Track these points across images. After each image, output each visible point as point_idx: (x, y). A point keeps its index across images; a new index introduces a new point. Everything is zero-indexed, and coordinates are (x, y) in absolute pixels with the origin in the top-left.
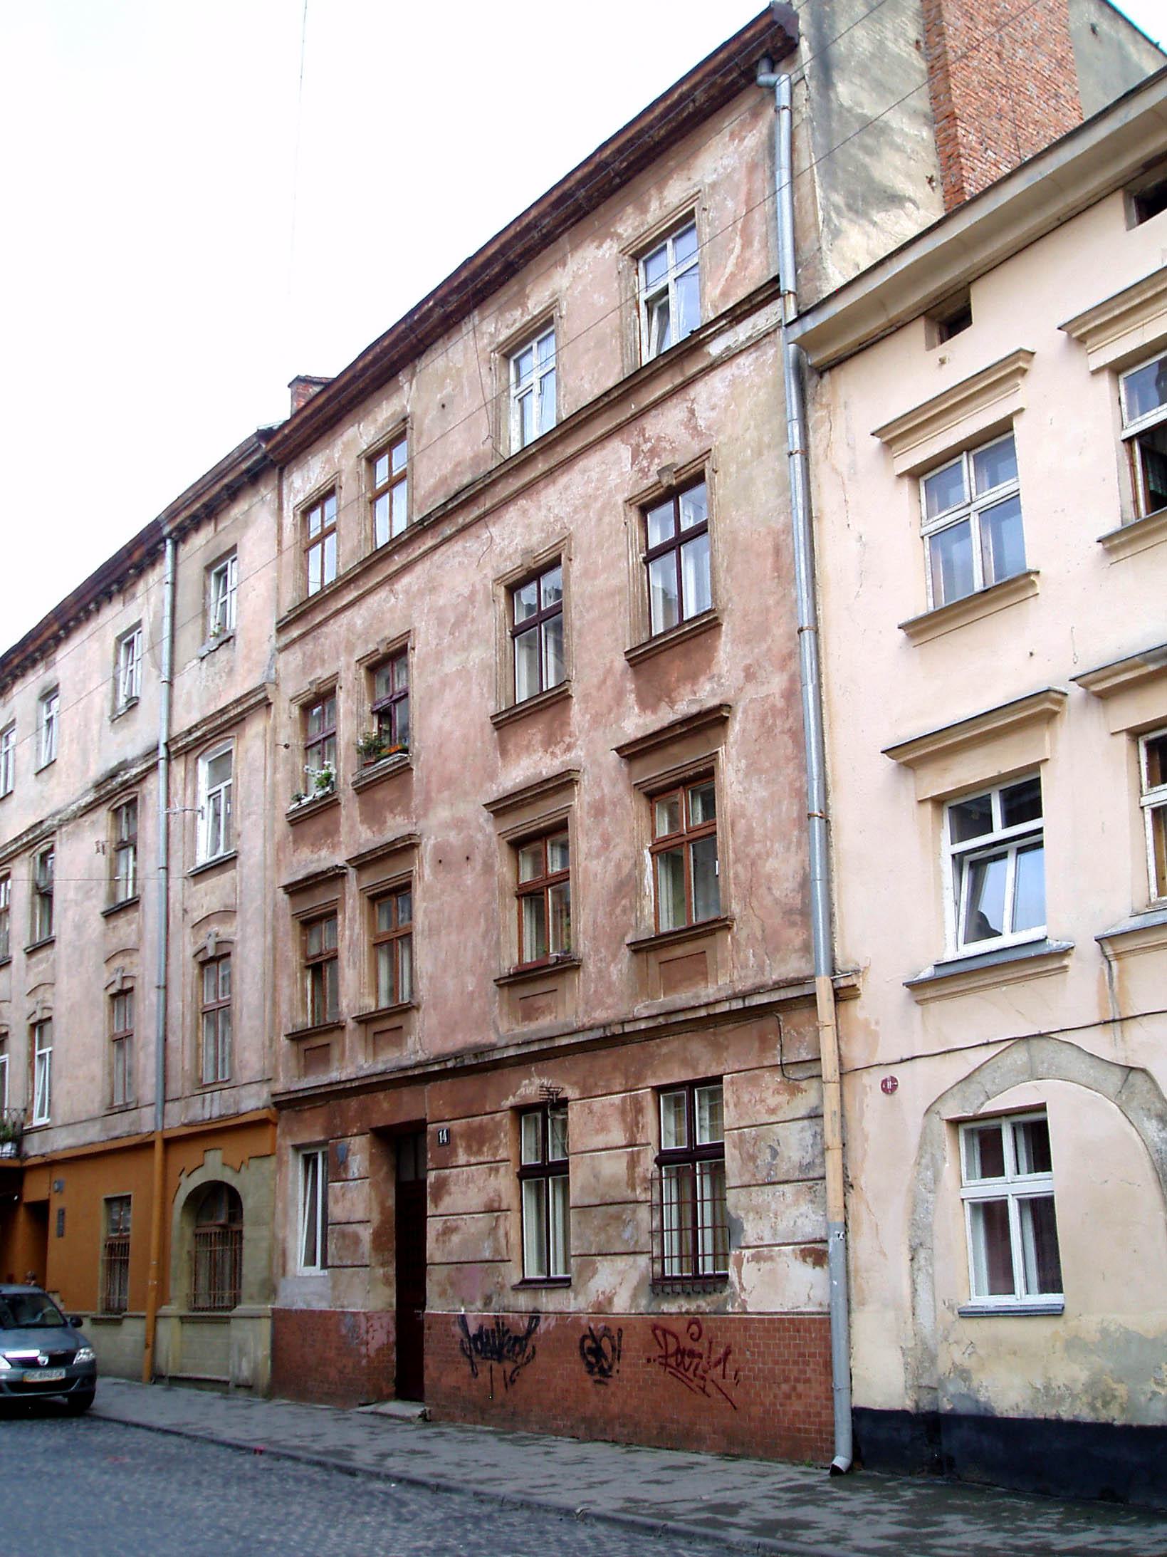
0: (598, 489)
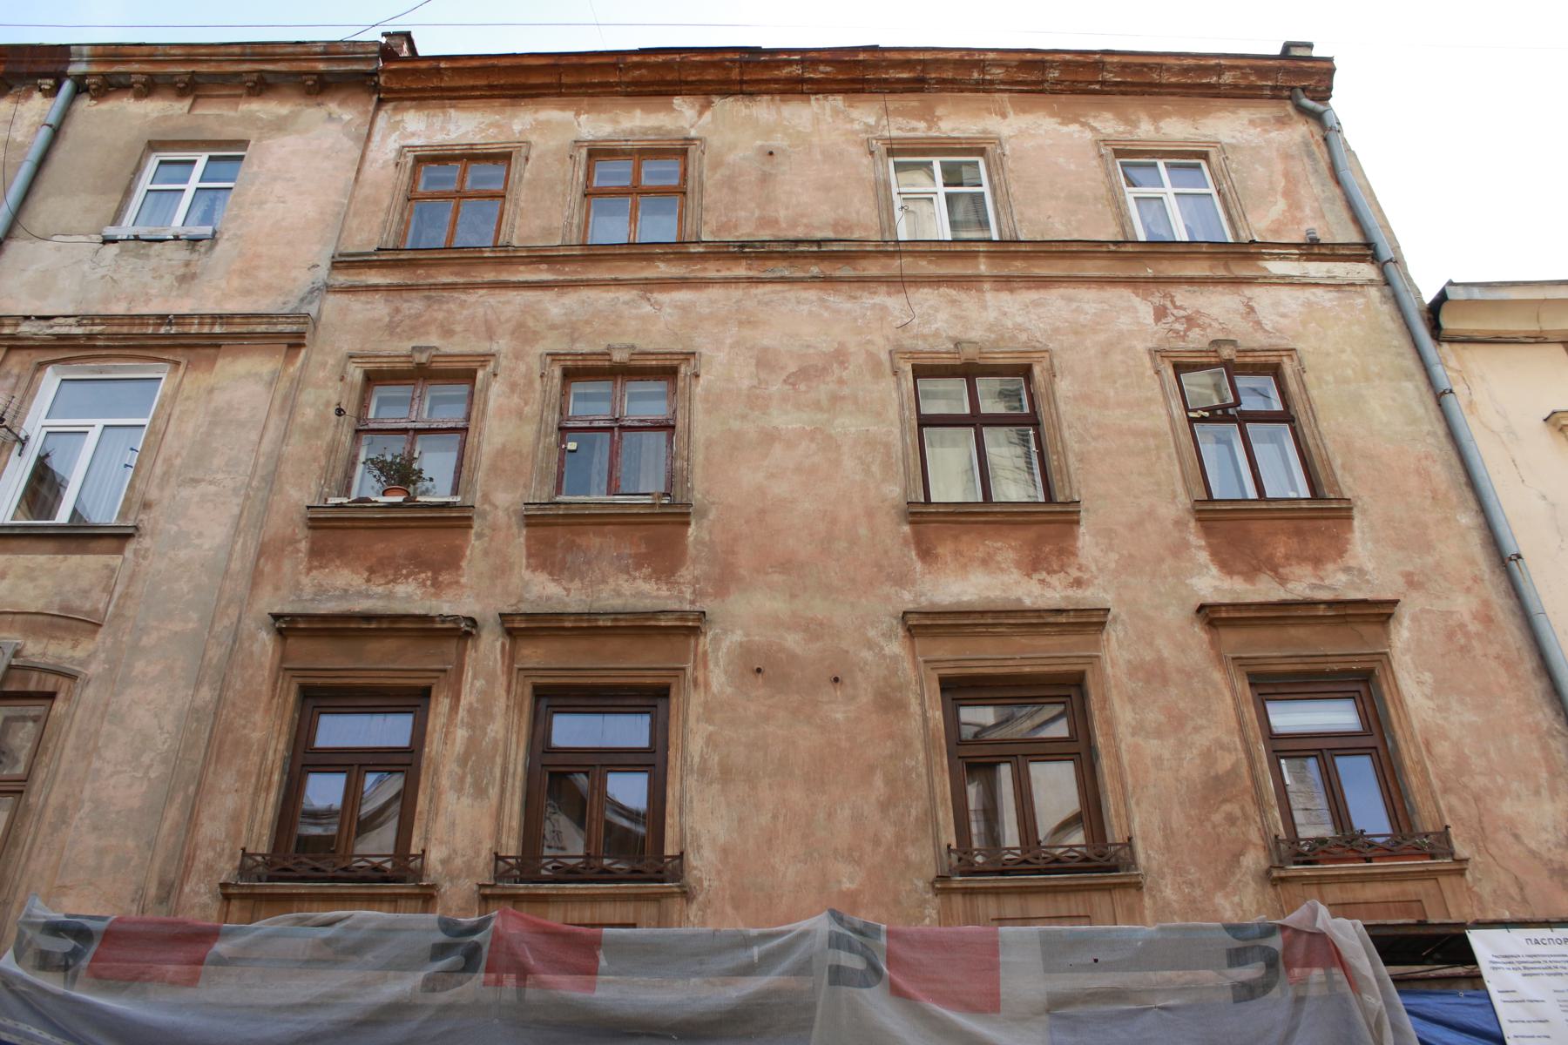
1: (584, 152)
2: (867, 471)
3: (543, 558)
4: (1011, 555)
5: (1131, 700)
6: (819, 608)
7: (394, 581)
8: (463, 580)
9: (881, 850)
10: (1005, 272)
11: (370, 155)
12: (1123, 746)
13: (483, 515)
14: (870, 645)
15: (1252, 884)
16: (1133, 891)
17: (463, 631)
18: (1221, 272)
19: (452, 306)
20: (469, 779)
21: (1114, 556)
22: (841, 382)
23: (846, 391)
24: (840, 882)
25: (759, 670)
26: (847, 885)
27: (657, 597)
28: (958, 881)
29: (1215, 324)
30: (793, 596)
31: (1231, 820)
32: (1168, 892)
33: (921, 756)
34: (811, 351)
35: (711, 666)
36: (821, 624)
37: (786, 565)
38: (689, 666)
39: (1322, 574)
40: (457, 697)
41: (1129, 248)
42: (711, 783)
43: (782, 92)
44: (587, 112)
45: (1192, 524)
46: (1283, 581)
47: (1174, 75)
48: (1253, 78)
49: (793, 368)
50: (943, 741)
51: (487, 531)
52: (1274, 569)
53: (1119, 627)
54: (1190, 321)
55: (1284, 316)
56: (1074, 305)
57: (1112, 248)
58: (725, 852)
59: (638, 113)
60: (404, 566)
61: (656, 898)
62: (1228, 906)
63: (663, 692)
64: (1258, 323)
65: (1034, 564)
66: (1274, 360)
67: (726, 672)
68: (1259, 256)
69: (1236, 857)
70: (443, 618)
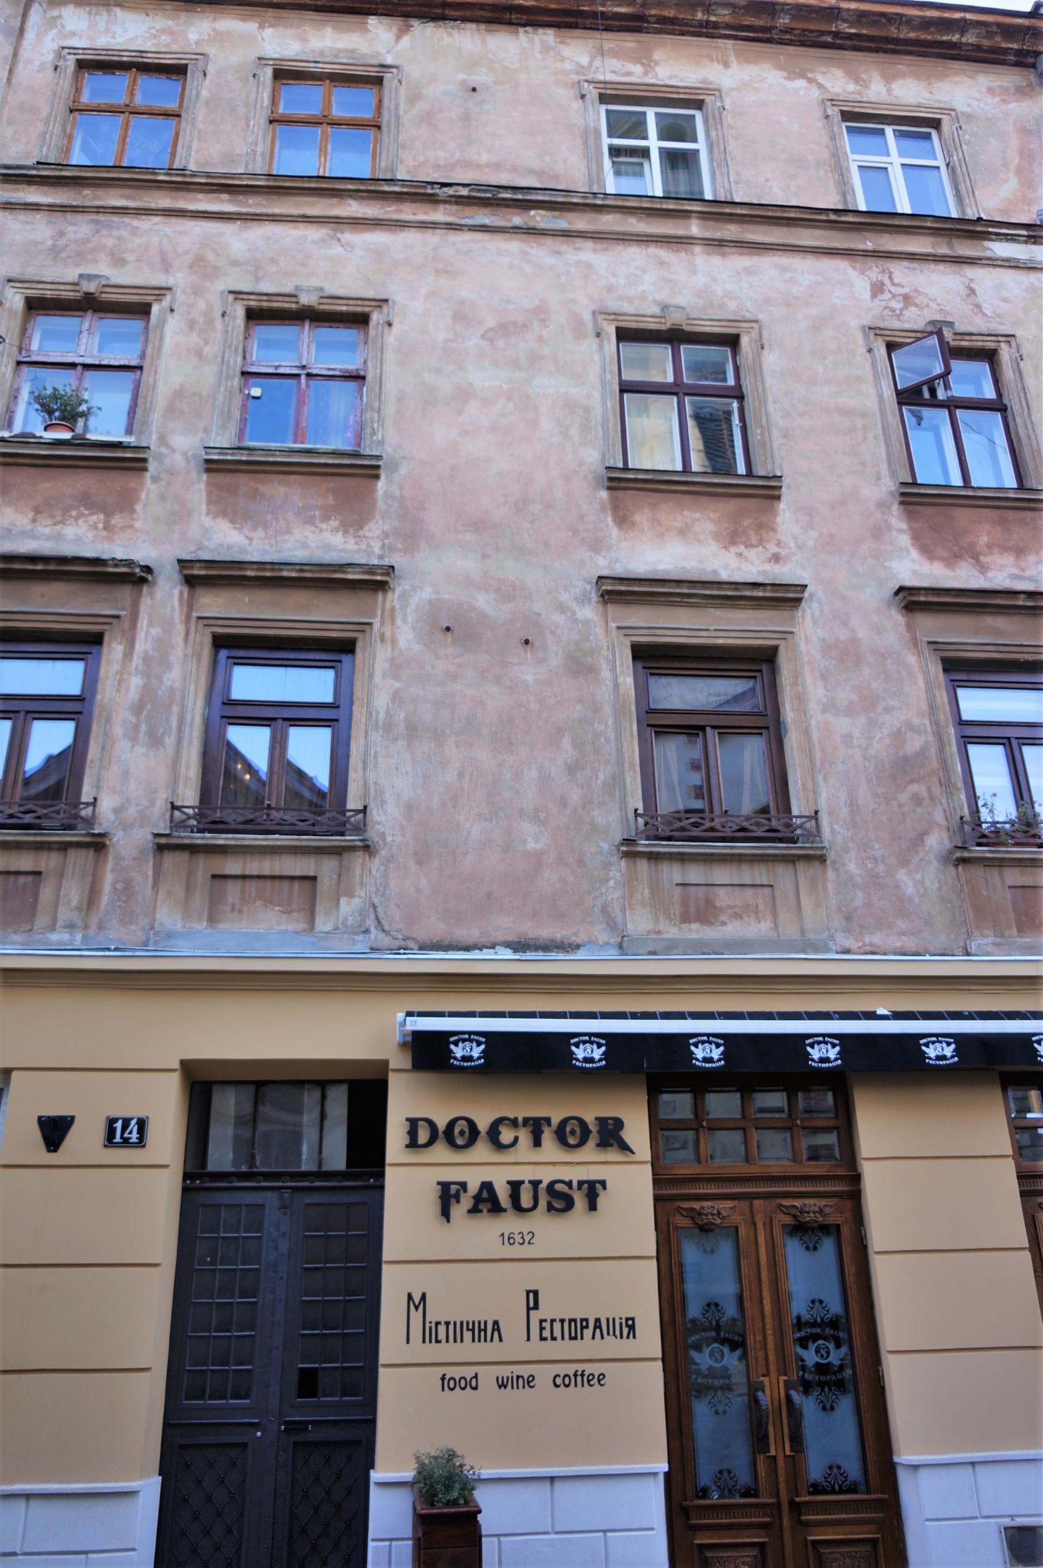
0: (811, 296)
1: (269, 72)
2: (565, 432)
3: (222, 505)
4: (710, 527)
5: (823, 678)
6: (511, 569)
7: (62, 522)
8: (138, 525)
9: (568, 812)
10: (718, 235)
11: (24, 54)
12: (813, 722)
13: (160, 458)
14: (562, 609)
15: (935, 863)
16: (817, 864)
17: (135, 577)
18: (943, 250)
19: (123, 233)
20: (143, 728)
21: (813, 534)
22: (540, 340)
23: (546, 350)
24: (525, 841)
25: (448, 629)
26: (531, 845)
27: (343, 551)
28: (643, 845)
29: (933, 305)
30: (485, 556)
31: (917, 800)
32: (852, 867)
33: (610, 722)
34: (511, 307)
35: (399, 622)
36: (514, 586)
37: (478, 525)
38: (376, 622)
39: (1023, 564)
40: (131, 644)
41: (850, 218)
42: (395, 739)
43: (489, 21)
44: (272, 26)
45: (895, 507)
46: (983, 569)
47: (913, 29)
48: (998, 39)
49: (491, 323)
50: (633, 708)
51: (163, 475)
52: (976, 557)
53: (815, 605)
54: (907, 299)
55: (1005, 300)
56: (788, 276)
57: (833, 217)
58: (410, 808)
59: (329, 31)
60: (73, 508)
61: (338, 852)
62: (910, 883)
63: (347, 647)
64: (978, 306)
65: (732, 538)
66: (991, 345)
67: (414, 629)
68: (985, 236)
69: (921, 837)
70: (117, 563)
